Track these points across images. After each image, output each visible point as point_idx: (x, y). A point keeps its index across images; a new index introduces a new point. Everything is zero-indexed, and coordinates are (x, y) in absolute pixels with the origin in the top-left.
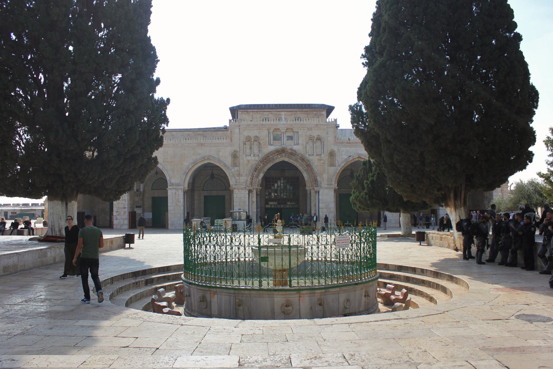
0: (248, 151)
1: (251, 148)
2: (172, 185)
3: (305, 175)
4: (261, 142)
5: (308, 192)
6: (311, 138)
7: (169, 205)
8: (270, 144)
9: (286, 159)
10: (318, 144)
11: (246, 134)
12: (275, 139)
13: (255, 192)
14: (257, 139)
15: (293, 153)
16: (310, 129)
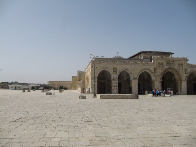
0: (159, 68)
1: (160, 67)
2: (134, 78)
3: (176, 77)
4: (164, 65)
5: (177, 82)
6: (179, 64)
7: (133, 86)
8: (166, 66)
9: (170, 71)
10: (181, 66)
11: (159, 62)
12: (168, 64)
13: (161, 82)
14: (162, 64)
15: (174, 69)
16: (179, 61)
